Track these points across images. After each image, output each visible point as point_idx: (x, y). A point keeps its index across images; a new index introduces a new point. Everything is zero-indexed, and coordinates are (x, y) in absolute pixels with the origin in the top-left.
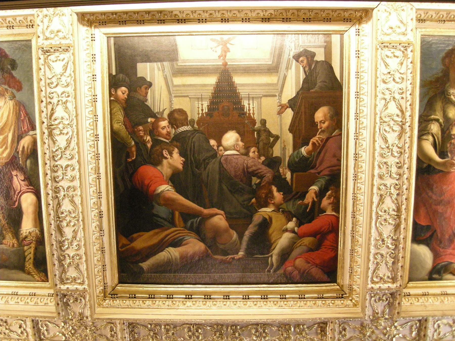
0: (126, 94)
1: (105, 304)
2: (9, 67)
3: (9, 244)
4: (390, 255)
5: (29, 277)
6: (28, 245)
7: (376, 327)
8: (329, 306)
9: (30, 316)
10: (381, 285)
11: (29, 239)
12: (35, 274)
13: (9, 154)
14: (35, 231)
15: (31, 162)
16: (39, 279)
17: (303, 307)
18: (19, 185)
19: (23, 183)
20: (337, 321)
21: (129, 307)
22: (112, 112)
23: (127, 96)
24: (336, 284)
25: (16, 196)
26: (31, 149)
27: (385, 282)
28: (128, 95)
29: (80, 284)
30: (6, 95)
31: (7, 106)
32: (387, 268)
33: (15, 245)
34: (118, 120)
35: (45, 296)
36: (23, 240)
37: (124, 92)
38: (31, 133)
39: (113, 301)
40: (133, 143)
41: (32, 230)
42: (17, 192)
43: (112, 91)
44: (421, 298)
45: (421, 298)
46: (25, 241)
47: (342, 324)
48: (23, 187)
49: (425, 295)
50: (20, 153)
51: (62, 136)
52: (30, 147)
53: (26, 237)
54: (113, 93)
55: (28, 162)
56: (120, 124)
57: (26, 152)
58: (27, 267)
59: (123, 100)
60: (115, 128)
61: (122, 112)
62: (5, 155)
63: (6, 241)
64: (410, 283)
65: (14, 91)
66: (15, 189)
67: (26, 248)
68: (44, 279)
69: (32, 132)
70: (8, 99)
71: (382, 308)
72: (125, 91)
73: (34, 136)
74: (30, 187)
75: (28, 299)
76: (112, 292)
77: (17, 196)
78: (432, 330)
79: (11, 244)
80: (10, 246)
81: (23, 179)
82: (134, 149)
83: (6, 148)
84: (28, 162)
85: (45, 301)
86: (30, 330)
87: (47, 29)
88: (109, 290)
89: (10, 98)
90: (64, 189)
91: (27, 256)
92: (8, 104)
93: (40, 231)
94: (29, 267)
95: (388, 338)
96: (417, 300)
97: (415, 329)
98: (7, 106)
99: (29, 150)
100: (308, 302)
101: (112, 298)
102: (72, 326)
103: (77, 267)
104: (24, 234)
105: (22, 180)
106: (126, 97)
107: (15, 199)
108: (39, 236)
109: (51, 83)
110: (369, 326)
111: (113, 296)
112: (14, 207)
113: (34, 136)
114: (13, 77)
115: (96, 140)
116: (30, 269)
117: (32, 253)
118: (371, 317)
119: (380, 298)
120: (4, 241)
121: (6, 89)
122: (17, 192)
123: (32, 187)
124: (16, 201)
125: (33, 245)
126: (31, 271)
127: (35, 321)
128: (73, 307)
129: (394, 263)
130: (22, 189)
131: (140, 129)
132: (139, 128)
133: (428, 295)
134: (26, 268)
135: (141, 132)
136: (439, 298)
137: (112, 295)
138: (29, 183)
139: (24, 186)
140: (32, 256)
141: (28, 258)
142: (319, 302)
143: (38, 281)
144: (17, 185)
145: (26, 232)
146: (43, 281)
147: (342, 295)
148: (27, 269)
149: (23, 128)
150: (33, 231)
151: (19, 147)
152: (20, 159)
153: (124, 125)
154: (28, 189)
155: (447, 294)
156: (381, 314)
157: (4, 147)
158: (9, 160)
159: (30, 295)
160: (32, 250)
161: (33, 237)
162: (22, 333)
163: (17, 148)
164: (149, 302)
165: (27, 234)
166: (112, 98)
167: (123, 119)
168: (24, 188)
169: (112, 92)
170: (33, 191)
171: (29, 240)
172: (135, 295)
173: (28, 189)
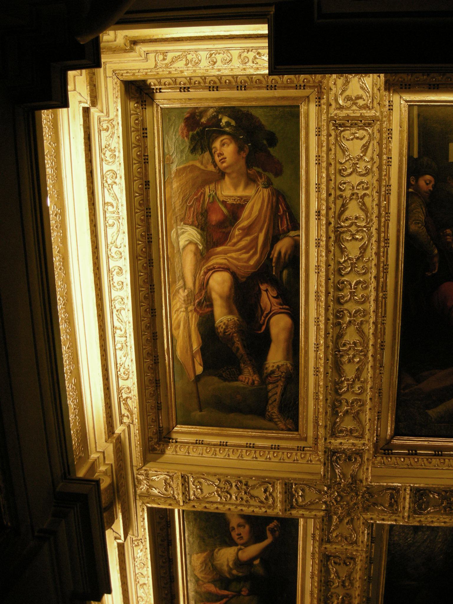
0: (431, 185)
1: (376, 462)
2: (265, 142)
5: (272, 424)
6: (275, 383)
9: (283, 479)
11: (276, 375)
12: (279, 421)
13: (258, 262)
14: (287, 364)
15: (289, 274)
16: (284, 427)
18: (269, 303)
21: (410, 466)
22: (409, 208)
23: (432, 187)
25: (263, 318)
26: (290, 255)
28: (434, 187)
29: (356, 437)
30: (259, 181)
31: (260, 196)
33: (256, 382)
34: (418, 220)
35: (293, 449)
36: (267, 377)
37: (428, 182)
38: (292, 233)
39: (387, 458)
40: (436, 251)
41: (282, 363)
42: (266, 313)
43: (411, 180)
46: (271, 377)
48: (274, 305)
50: (274, 260)
51: (354, 242)
52: (289, 252)
53: (273, 372)
54: (413, 183)
55: (285, 272)
56: (420, 225)
57: (282, 260)
58: (269, 412)
59: (426, 193)
60: (411, 230)
61: (424, 209)
62: (252, 263)
63: (243, 376)
65: (271, 176)
66: (263, 308)
67: (270, 387)
68: (290, 427)
69: (294, 232)
70: (260, 187)
72: (430, 181)
73: (296, 238)
74: (284, 306)
75: (269, 453)
76: (386, 446)
77: (265, 318)
79: (250, 381)
80: (248, 384)
81: (275, 296)
82: (436, 259)
83: (255, 253)
84: (285, 272)
85: (294, 457)
86: (279, 496)
87: (341, 94)
88: (382, 444)
89: (265, 185)
90: (350, 314)
91: (271, 397)
92: (261, 193)
93: (292, 365)
94: (273, 411)
98: (260, 196)
99: (287, 257)
101: (385, 454)
102: (337, 492)
103: (356, 417)
104: (270, 369)
106: (431, 189)
107: (261, 322)
108: (291, 372)
109: (343, 169)
111: (386, 451)
112: (260, 332)
113: (296, 238)
114: (269, 155)
115: (386, 247)
116: (273, 414)
120: (240, 377)
121: (258, 172)
122: (266, 313)
123: (287, 307)
124: (264, 324)
125: (281, 383)
126: (275, 417)
127: (288, 485)
128: (344, 468)
130: (273, 309)
131: (448, 232)
132: (446, 232)
134: (267, 413)
135: (448, 237)
137: (385, 450)
138: (283, 302)
139: (275, 304)
140: (277, 397)
141: (273, 399)
143: (282, 430)
144: (266, 304)
145: (273, 366)
146: (289, 430)
148: (270, 414)
149: (281, 227)
150: (282, 365)
151: (272, 252)
152: (274, 268)
153: (424, 226)
154: (281, 309)
157: (251, 252)
158: (257, 270)
159: (272, 448)
160: (279, 390)
161: (282, 373)
162: (267, 499)
163: (270, 254)
164: (435, 461)
165: (274, 368)
166: (410, 190)
167: (424, 218)
168: (276, 308)
169: (412, 182)
171: (275, 377)
172: (416, 451)
173: (281, 309)
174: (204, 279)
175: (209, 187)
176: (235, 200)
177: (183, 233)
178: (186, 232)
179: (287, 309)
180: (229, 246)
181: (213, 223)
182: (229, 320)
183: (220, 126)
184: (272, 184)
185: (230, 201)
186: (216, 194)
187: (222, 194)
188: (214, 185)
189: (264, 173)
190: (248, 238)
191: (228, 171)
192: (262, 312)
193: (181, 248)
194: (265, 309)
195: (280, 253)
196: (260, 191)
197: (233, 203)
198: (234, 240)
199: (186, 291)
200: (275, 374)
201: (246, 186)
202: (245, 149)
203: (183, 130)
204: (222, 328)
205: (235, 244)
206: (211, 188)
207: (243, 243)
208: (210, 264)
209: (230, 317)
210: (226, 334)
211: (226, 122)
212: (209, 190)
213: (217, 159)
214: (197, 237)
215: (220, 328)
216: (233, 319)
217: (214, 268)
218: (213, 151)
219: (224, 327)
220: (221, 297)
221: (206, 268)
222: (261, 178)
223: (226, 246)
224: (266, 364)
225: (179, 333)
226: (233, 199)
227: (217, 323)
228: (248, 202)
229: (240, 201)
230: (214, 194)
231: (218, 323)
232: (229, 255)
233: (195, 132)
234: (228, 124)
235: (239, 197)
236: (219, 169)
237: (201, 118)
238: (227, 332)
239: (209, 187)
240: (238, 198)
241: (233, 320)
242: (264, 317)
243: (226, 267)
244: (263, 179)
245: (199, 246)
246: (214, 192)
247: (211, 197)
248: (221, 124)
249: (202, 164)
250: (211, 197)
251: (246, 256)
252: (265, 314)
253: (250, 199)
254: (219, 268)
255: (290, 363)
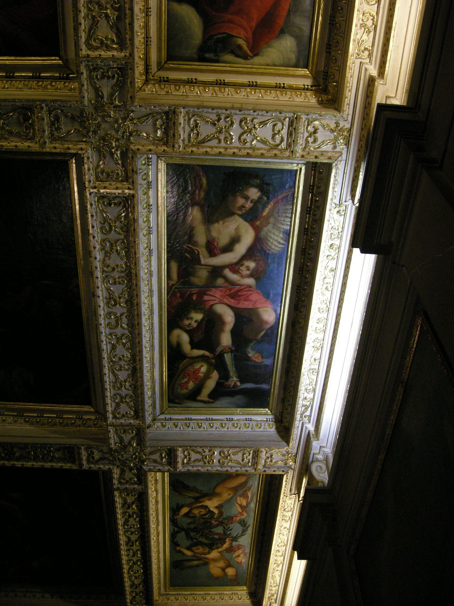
4: (112, 6)
7: (103, 117)
8: (47, 89)
10: (103, 53)
17: (9, 89)
20: (44, 105)
24: (57, 58)
27: (108, 48)
32: (109, 27)
44: (184, 86)
45: (184, 86)
47: (53, 111)
49: (192, 82)
64: (169, 62)
71: (109, 89)
78: (187, 129)
95: (123, 137)
96: (177, 88)
97: (161, 126)
100: (18, 82)
110: (92, 116)
118: (93, 102)
119: (103, 73)
129: (119, 18)
133: (196, 83)
136: (211, 88)
142: (33, 83)
147: (68, 75)
155: (224, 84)
156: (108, 99)
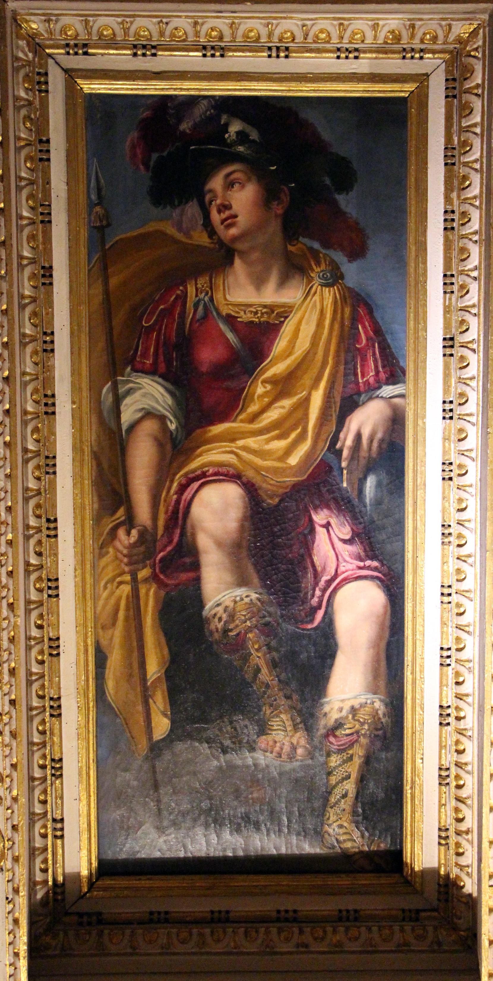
2: (328, 181)
3: (277, 749)
6: (344, 750)
11: (348, 732)
13: (309, 456)
14: (373, 703)
15: (379, 485)
18: (332, 554)
19: (346, 550)
25: (318, 593)
26: (382, 441)
30: (313, 270)
31: (315, 305)
33: (300, 751)
36: (327, 736)
38: (388, 390)
41: (362, 700)
42: (325, 578)
46: (335, 736)
48: (345, 561)
50: (345, 453)
52: (379, 435)
53: (339, 725)
55: (370, 482)
57: (364, 453)
62: (294, 460)
63: (270, 738)
65: (339, 257)
66: (319, 569)
67: (334, 761)
69: (391, 387)
70: (316, 282)
73: (396, 400)
74: (368, 563)
75: (335, 932)
77: (324, 591)
79: (287, 748)
80: (279, 755)
81: (347, 537)
83: (302, 437)
84: (370, 482)
89: (326, 279)
91: (334, 787)
92: (317, 298)
93: (386, 705)
98: (315, 305)
99: (375, 444)
104: (334, 716)
105: (344, 541)
107: (315, 600)
108: (383, 720)
112: (310, 626)
113: (396, 400)
114: (339, 213)
117: (354, 776)
120: (263, 742)
121: (311, 249)
122: (325, 578)
123: (375, 564)
124: (319, 607)
125: (358, 752)
130: (342, 569)
138: (365, 551)
139: (348, 559)
140: (350, 786)
141: (338, 792)
144: (327, 557)
145: (341, 710)
149: (363, 376)
150: (362, 706)
151: (342, 435)
152: (345, 472)
154: (360, 568)
157: (293, 435)
158: (306, 477)
159: (340, 919)
160: (354, 768)
161: (362, 724)
163: (335, 439)
165: (344, 713)
168: (350, 567)
170: (375, 574)
171: (347, 735)
173: (360, 568)
174: (178, 502)
175: (196, 284)
176: (256, 313)
177: (129, 392)
178: (140, 389)
179: (376, 569)
180: (242, 421)
181: (204, 369)
182: (238, 599)
183: (225, 140)
184: (342, 277)
185: (245, 317)
186: (212, 299)
187: (226, 299)
188: (207, 278)
189: (324, 251)
190: (287, 403)
191: (239, 246)
192: (317, 576)
193: (124, 427)
194: (324, 569)
195: (358, 436)
196: (315, 293)
197: (252, 322)
198: (253, 408)
199: (134, 532)
200: (345, 730)
201: (283, 282)
202: (282, 196)
203: (133, 147)
204: (220, 619)
205: (254, 418)
206: (199, 286)
207: (273, 415)
208: (194, 465)
209: (241, 592)
210: (231, 634)
211: (238, 133)
212: (197, 289)
213: (216, 217)
214: (165, 401)
215: (216, 620)
216: (247, 596)
217: (204, 475)
218: (207, 198)
219: (225, 617)
220: (219, 544)
221: (186, 474)
222: (318, 264)
223: (234, 421)
224: (322, 705)
225: (112, 636)
226: (251, 312)
227: (207, 607)
228: (286, 317)
229: (269, 317)
230: (206, 299)
231: (211, 609)
232: (240, 443)
233: (165, 154)
234: (242, 136)
235: (265, 306)
236: (221, 242)
237: (180, 121)
238: (231, 630)
239: (196, 284)
240: (264, 310)
241: (247, 600)
242: (320, 589)
243: (232, 471)
244: (323, 267)
245: (169, 423)
246: (207, 294)
247: (201, 308)
248: (227, 136)
249: (180, 229)
250: (201, 308)
251: (282, 444)
252: (322, 583)
253: (291, 312)
254: (215, 474)
255: (381, 700)
